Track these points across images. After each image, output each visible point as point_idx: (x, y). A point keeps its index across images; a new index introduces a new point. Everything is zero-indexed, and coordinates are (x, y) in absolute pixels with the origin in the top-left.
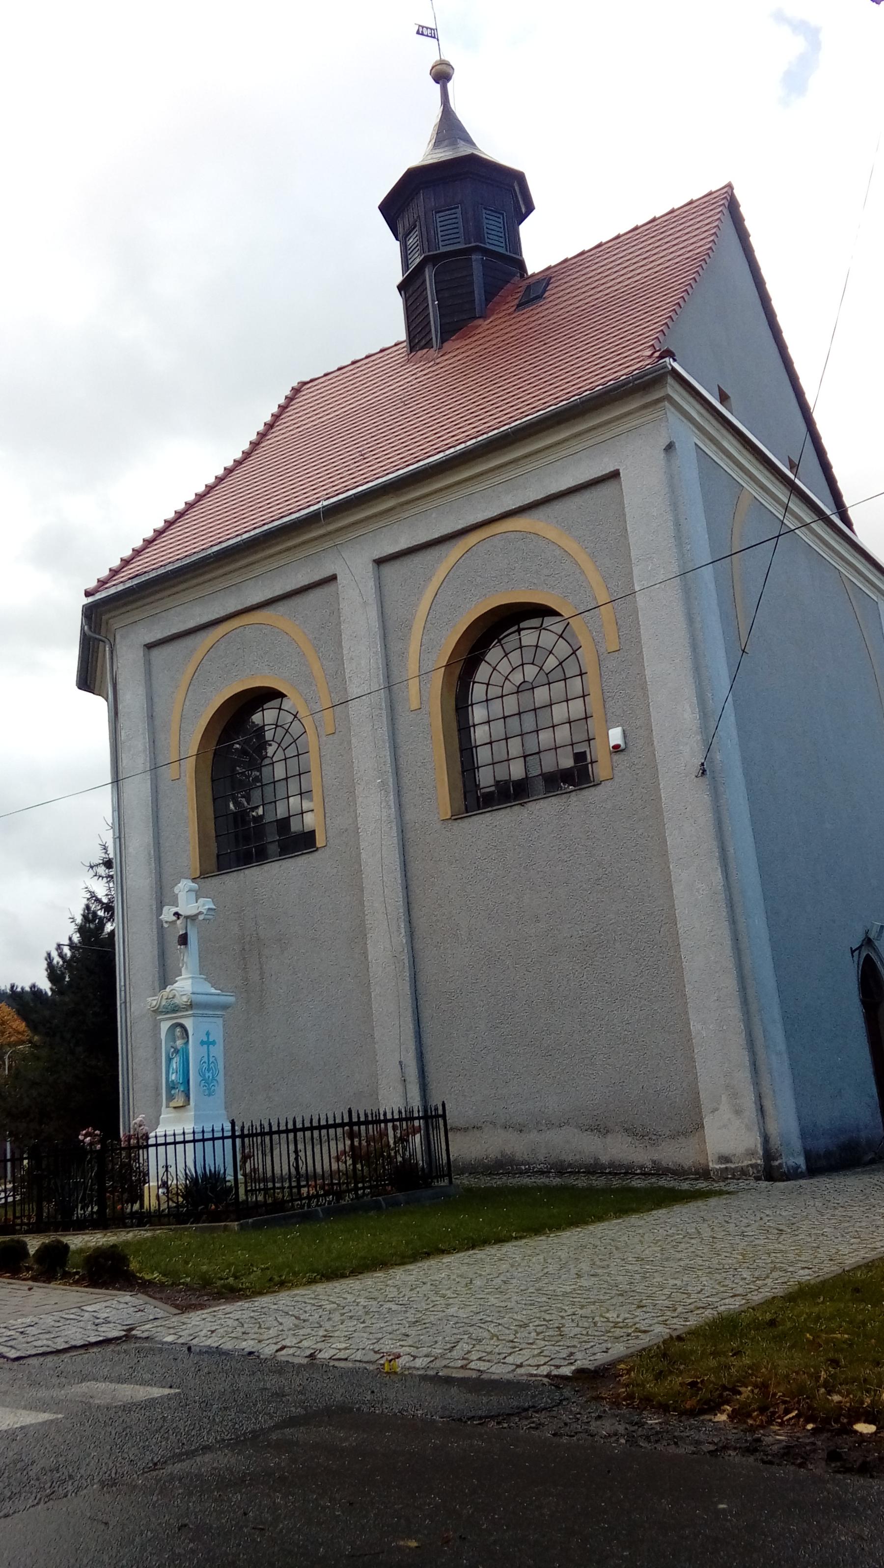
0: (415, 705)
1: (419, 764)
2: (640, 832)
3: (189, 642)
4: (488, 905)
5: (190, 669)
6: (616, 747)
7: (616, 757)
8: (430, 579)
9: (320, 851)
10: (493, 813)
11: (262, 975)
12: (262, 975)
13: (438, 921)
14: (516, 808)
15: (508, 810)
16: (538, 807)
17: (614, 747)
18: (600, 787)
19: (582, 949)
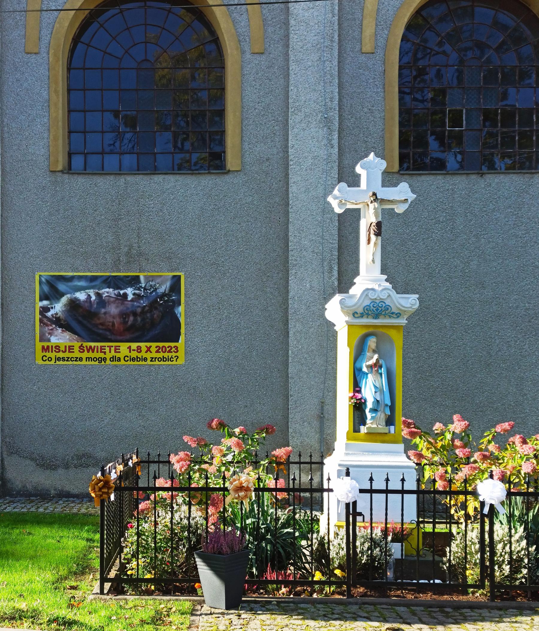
0: (367, 47)
4: (429, 264)
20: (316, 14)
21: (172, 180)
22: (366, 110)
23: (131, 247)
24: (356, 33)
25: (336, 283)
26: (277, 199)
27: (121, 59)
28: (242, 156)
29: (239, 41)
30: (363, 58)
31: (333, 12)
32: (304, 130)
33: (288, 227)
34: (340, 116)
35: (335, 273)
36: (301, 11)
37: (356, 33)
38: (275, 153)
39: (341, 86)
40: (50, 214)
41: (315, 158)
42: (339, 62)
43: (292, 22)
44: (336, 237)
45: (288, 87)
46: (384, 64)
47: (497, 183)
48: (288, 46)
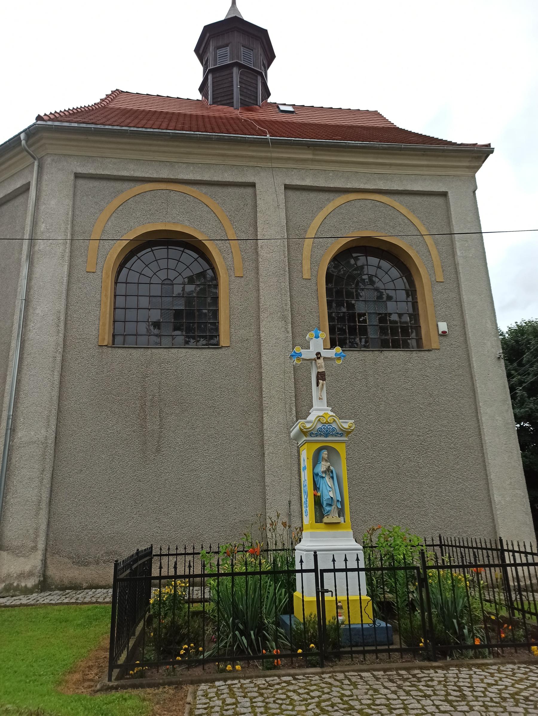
3: (118, 185)
5: (117, 202)
6: (444, 332)
8: (322, 208)
9: (223, 349)
10: (360, 352)
14: (376, 352)
15: (371, 353)
19: (419, 443)
20: (274, 256)
21: (184, 351)
23: (154, 396)
24: (299, 268)
26: (254, 364)
27: (151, 278)
29: (228, 269)
30: (304, 282)
31: (284, 254)
33: (261, 382)
34: (292, 314)
35: (294, 412)
36: (265, 254)
37: (299, 268)
38: (252, 335)
39: (291, 296)
40: (97, 373)
41: (277, 339)
43: (260, 260)
44: (293, 389)
45: (259, 297)
46: (317, 285)
47: (391, 357)
48: (258, 274)
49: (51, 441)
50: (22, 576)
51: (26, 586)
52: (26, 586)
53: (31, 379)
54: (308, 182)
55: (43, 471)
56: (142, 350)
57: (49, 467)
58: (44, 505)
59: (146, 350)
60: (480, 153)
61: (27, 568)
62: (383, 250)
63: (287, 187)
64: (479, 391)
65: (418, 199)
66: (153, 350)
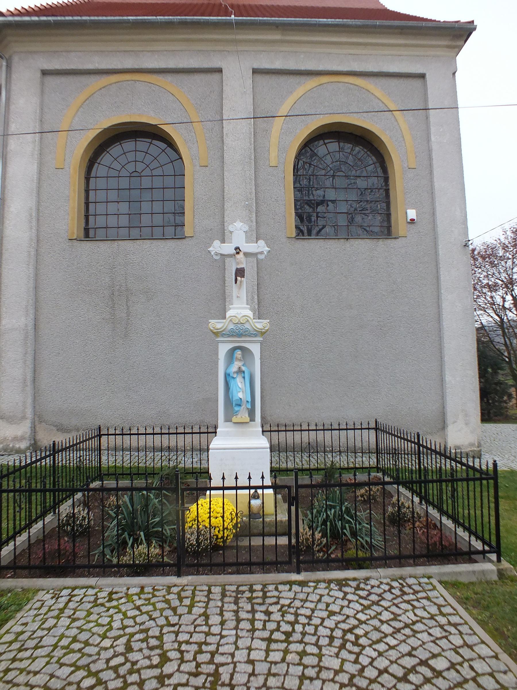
1: (273, 200)
2: (421, 269)
4: (317, 294)
6: (412, 220)
7: (409, 225)
9: (187, 239)
11: (128, 314)
12: (128, 314)
13: (279, 298)
16: (357, 243)
17: (411, 220)
18: (397, 240)
22: (273, 200)
25: (257, 307)
28: (194, 228)
32: (233, 211)
35: (256, 301)
39: (256, 185)
42: (255, 172)
43: (225, 148)
48: (223, 162)
49: (30, 327)
50: (15, 439)
51: (19, 448)
52: (19, 448)
53: (10, 272)
54: (278, 65)
55: (26, 354)
56: (109, 242)
57: (30, 351)
58: (29, 383)
59: (113, 242)
60: (459, 33)
61: (19, 433)
62: (356, 136)
63: (255, 71)
64: (442, 278)
65: (394, 82)
66: (120, 242)
